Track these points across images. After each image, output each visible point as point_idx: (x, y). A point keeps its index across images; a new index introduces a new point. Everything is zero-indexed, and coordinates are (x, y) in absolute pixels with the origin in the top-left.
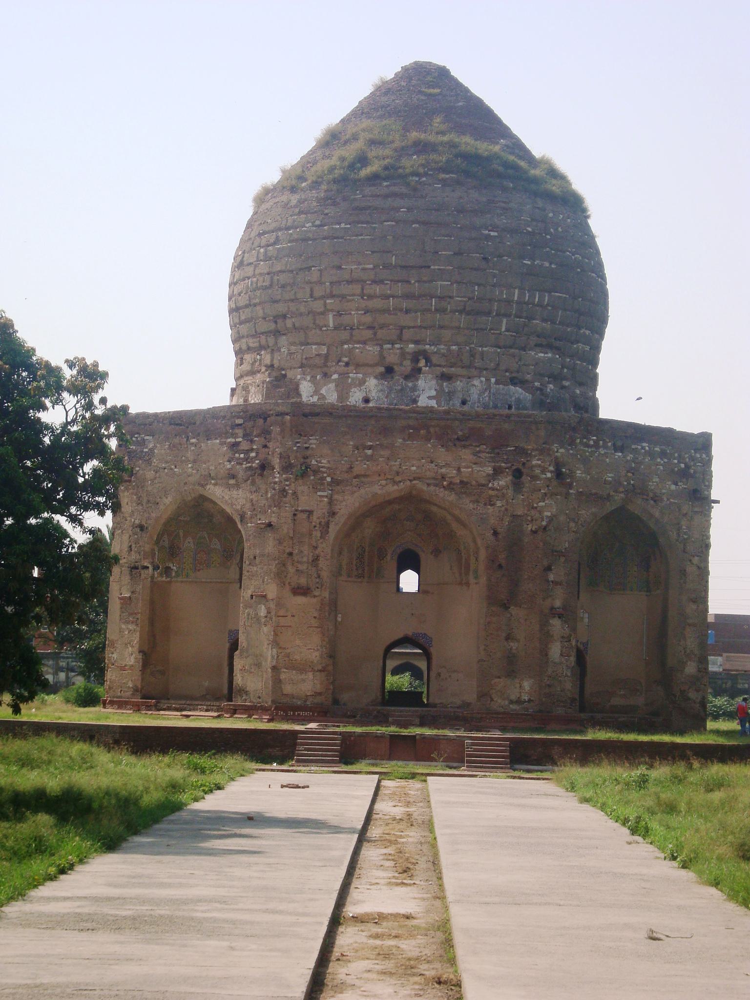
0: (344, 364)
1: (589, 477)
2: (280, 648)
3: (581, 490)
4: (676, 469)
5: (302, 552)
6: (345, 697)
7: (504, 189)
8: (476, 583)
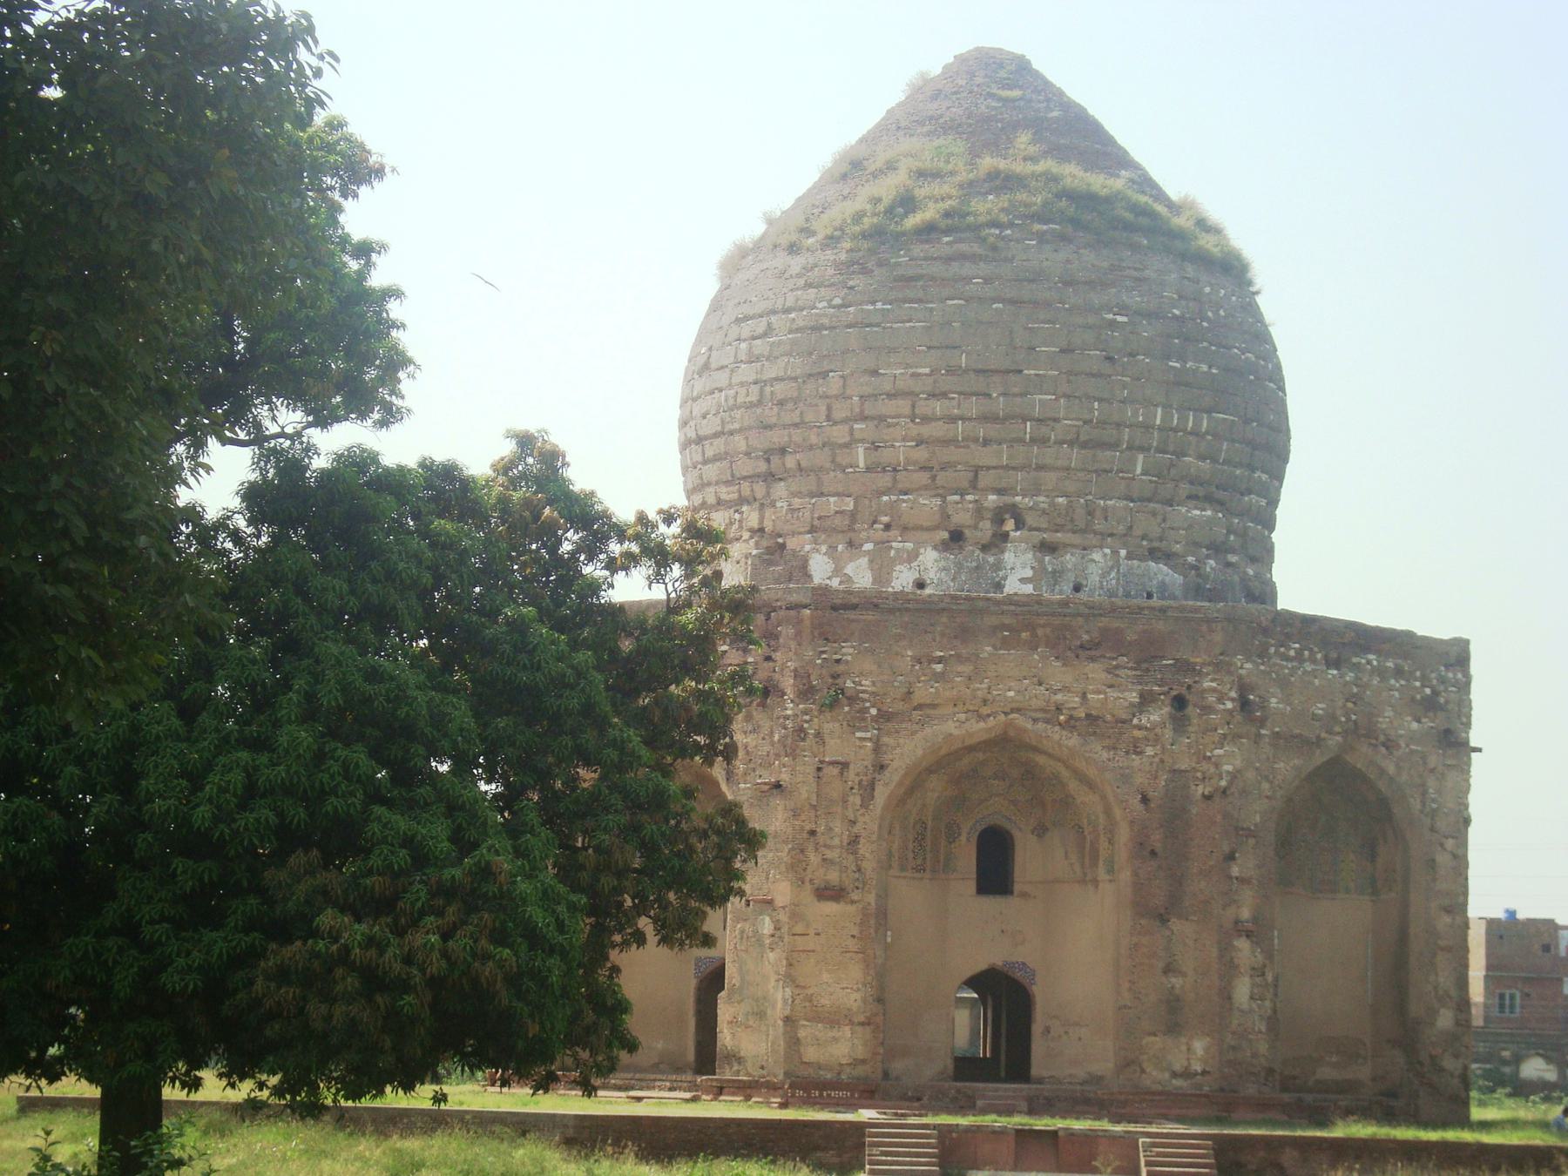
0: (882, 526)
1: (1289, 708)
2: (797, 986)
3: (1277, 729)
4: (1418, 697)
5: (831, 829)
6: (898, 1066)
7: (1135, 247)
8: (1110, 881)
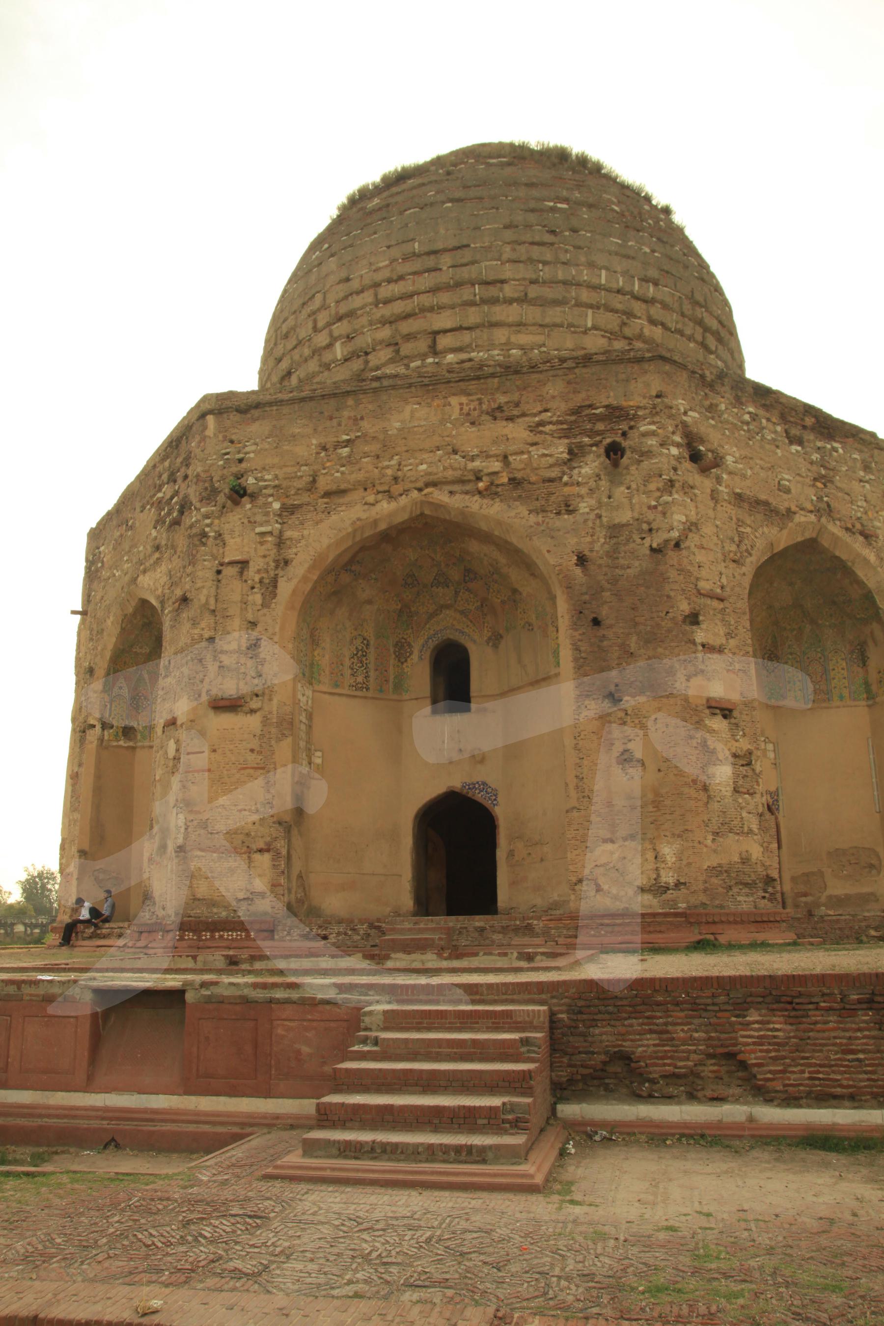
2: (191, 812)
3: (738, 491)
